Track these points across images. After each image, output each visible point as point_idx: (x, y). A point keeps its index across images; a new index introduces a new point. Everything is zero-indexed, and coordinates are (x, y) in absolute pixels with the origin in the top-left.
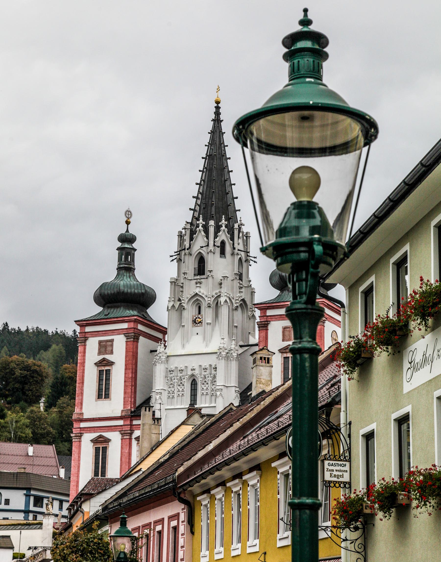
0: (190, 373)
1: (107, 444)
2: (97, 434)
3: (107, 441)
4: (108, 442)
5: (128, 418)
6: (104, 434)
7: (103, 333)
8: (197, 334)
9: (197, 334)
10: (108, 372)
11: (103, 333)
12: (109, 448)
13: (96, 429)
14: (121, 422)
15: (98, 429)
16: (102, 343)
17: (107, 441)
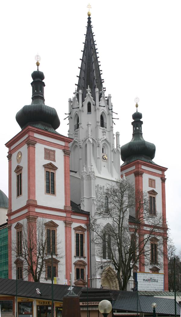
0: (105, 191)
1: (55, 228)
2: (50, 220)
3: (56, 226)
4: (56, 227)
5: (70, 212)
6: (54, 221)
7: (48, 143)
8: (104, 166)
9: (104, 166)
10: (53, 174)
11: (48, 143)
12: (57, 232)
13: (47, 215)
14: (64, 215)
15: (49, 216)
16: (47, 151)
17: (56, 226)
